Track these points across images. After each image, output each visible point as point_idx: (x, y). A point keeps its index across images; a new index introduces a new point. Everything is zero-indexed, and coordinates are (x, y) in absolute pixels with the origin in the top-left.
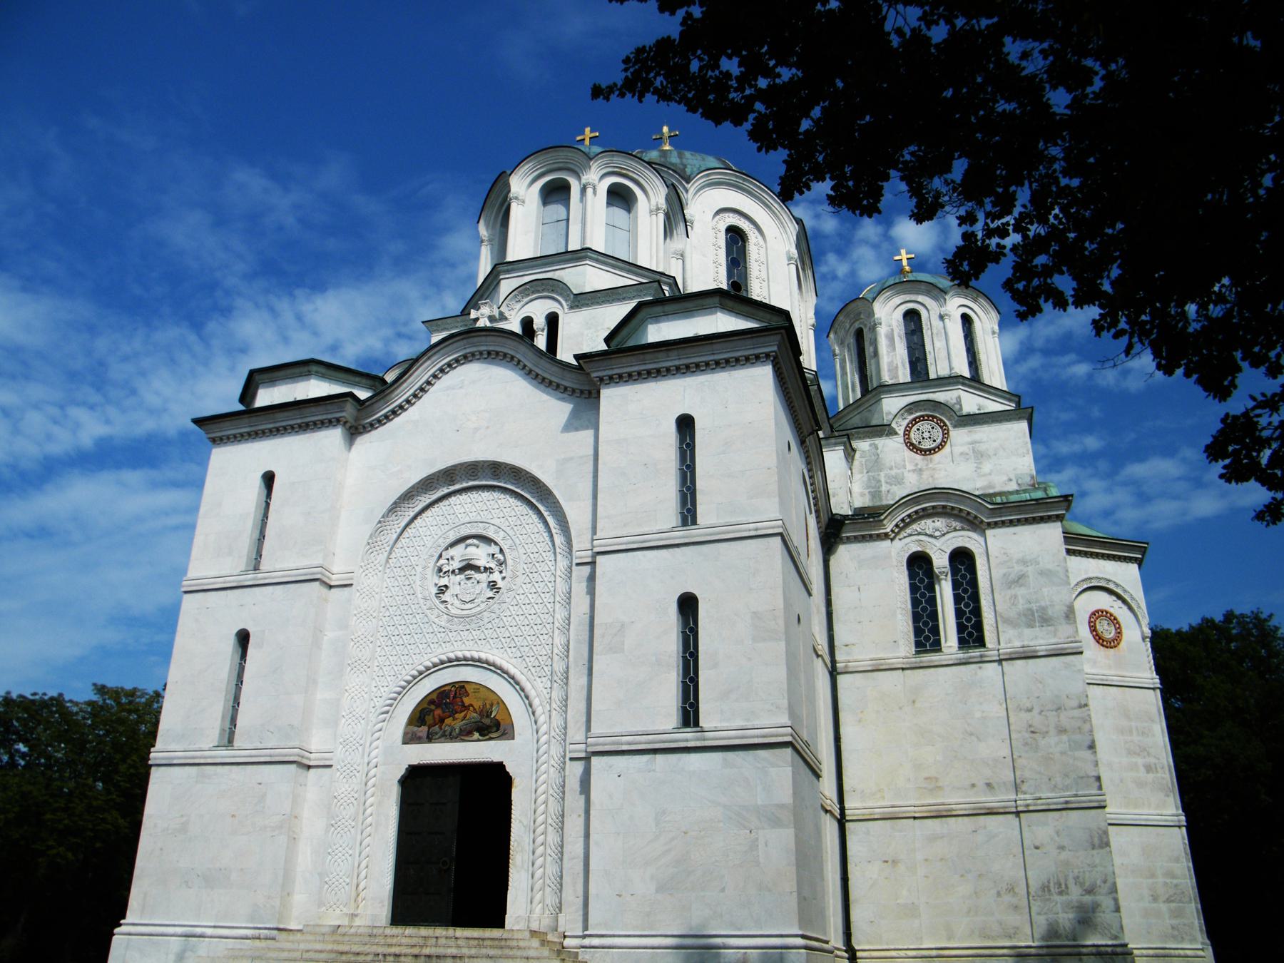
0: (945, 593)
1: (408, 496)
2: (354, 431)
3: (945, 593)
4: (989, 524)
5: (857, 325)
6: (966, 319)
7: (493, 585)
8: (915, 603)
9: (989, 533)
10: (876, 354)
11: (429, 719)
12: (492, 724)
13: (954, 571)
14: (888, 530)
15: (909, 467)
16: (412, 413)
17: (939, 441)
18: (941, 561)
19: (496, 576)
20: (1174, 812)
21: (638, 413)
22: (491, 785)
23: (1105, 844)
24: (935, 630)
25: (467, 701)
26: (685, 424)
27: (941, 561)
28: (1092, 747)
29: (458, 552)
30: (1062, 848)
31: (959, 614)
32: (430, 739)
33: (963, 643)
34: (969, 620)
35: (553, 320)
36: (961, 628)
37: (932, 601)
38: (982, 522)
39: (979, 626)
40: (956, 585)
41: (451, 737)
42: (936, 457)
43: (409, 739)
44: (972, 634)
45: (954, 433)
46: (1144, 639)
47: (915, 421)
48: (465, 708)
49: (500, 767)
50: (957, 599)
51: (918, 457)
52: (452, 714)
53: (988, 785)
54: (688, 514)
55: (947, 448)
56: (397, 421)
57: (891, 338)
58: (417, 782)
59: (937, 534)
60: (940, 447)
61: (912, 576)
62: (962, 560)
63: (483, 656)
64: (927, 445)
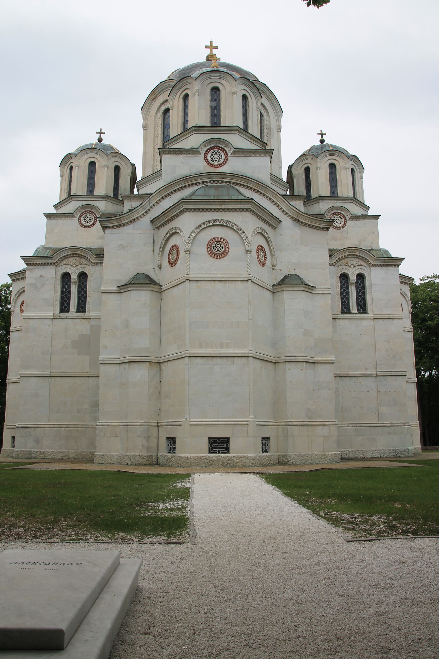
0: (353, 291)
3: (353, 291)
4: (373, 264)
6: (353, 170)
8: (342, 293)
9: (372, 268)
13: (357, 282)
14: (334, 262)
17: (342, 224)
18: (353, 278)
20: (413, 377)
24: (348, 305)
27: (353, 278)
31: (358, 299)
33: (358, 310)
34: (361, 302)
36: (358, 305)
37: (348, 293)
38: (370, 263)
39: (365, 305)
40: (357, 288)
44: (362, 307)
45: (349, 222)
46: (409, 312)
50: (357, 293)
55: (345, 227)
59: (352, 266)
60: (343, 227)
62: (361, 277)
64: (338, 225)
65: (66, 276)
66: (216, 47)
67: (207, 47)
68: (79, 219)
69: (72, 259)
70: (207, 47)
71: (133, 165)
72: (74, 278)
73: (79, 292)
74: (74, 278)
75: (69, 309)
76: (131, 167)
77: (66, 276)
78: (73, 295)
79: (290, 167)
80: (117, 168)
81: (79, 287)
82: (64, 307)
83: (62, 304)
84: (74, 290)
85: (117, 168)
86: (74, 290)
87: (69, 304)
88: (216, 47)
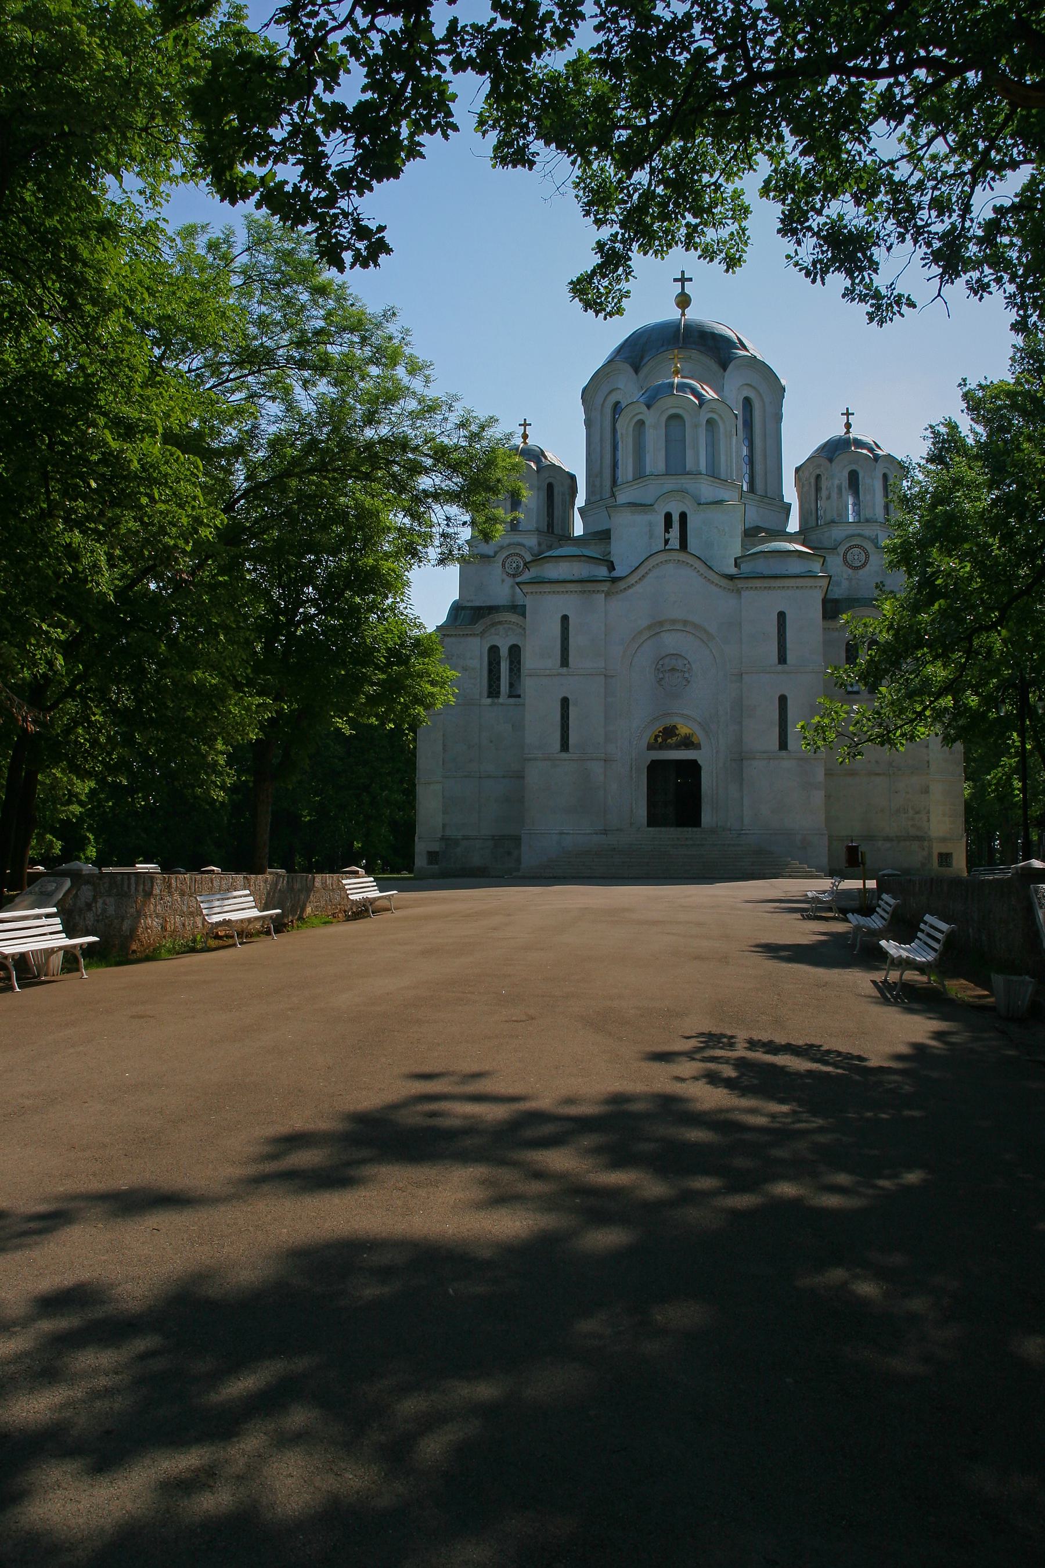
1: (640, 633)
2: (608, 594)
5: (818, 472)
7: (687, 679)
10: (829, 498)
11: (660, 740)
12: (688, 743)
15: (845, 576)
16: (638, 588)
19: (686, 675)
21: (761, 606)
22: (692, 768)
23: (926, 791)
25: (677, 732)
26: (782, 615)
28: (927, 747)
29: (667, 660)
30: (907, 793)
32: (661, 747)
35: (683, 516)
41: (670, 747)
42: (861, 572)
43: (650, 747)
47: (851, 547)
48: (677, 735)
49: (695, 762)
51: (850, 571)
52: (671, 737)
53: (877, 762)
54: (782, 659)
56: (631, 591)
57: (840, 488)
58: (655, 769)
60: (864, 565)
61: (847, 651)
63: (685, 712)
65: (494, 650)
66: (690, 280)
67: (675, 280)
68: (503, 565)
69: (501, 627)
70: (675, 280)
71: (573, 478)
72: (504, 652)
73: (511, 670)
74: (504, 652)
75: (499, 692)
76: (569, 481)
77: (494, 650)
78: (503, 673)
79: (797, 470)
80: (550, 487)
81: (511, 663)
82: (493, 692)
83: (490, 686)
84: (504, 666)
85: (550, 487)
86: (504, 666)
87: (499, 686)
88: (690, 280)
